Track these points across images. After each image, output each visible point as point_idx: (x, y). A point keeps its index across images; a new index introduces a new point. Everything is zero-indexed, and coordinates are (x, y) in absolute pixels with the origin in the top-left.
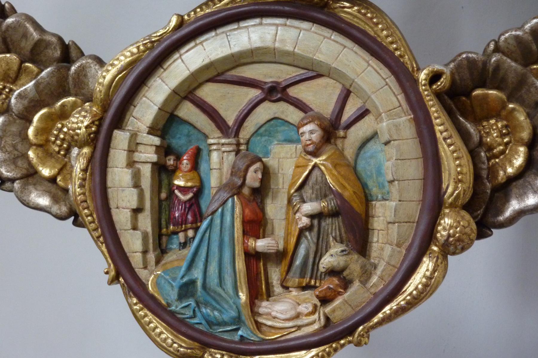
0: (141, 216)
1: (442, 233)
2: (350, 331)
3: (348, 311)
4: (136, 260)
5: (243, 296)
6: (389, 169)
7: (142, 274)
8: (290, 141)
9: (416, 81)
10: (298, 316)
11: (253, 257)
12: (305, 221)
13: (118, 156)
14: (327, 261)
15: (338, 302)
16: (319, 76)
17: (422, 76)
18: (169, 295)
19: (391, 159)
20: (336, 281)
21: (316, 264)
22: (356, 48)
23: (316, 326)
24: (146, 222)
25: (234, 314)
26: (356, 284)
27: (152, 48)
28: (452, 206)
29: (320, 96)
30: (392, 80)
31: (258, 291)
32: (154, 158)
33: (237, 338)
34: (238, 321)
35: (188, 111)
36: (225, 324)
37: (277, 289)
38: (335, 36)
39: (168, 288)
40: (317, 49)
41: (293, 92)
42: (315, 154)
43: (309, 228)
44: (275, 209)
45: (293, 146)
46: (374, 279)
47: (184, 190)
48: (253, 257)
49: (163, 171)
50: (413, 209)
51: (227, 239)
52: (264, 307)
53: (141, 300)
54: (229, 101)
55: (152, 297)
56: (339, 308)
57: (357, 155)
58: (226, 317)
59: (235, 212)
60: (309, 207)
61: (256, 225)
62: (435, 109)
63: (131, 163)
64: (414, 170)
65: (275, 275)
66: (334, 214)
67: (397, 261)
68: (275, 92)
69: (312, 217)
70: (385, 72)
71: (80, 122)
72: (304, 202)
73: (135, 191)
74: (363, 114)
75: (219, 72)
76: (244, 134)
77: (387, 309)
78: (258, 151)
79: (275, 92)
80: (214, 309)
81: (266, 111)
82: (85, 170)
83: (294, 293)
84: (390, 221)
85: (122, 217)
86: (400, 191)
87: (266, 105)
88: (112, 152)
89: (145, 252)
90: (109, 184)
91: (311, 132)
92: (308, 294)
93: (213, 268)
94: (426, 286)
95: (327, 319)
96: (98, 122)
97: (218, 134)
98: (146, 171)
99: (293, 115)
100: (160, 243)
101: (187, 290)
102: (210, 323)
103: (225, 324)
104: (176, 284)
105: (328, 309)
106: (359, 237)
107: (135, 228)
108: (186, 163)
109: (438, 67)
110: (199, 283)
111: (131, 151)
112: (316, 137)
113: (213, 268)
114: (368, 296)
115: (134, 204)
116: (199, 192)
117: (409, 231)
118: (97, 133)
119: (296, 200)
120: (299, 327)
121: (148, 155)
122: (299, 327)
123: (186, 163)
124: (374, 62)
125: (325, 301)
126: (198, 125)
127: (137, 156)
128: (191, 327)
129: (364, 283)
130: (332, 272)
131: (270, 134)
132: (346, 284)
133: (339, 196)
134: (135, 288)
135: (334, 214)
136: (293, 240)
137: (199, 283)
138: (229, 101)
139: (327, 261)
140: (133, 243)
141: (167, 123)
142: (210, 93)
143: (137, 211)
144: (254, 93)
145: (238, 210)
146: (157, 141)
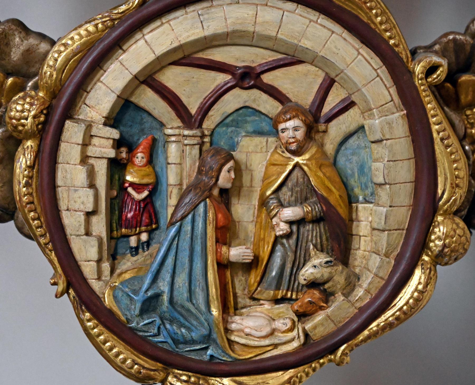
0: (94, 219)
1: (436, 244)
2: (333, 349)
3: (331, 328)
4: (89, 270)
5: (215, 312)
6: (378, 171)
7: (96, 285)
8: (260, 133)
9: (411, 73)
10: (272, 333)
11: (223, 266)
12: (283, 228)
13: (70, 150)
14: (308, 272)
15: (319, 317)
16: (300, 62)
17: (419, 69)
18: (127, 310)
19: (385, 160)
20: (317, 294)
21: (294, 275)
22: (346, 34)
23: (295, 344)
24: (99, 225)
25: (205, 332)
26: (340, 298)
27: (113, 28)
28: (445, 213)
29: (299, 84)
30: (383, 72)
31: (229, 306)
32: (112, 153)
33: (206, 358)
34: (208, 339)
35: (148, 99)
36: (193, 342)
37: (242, 301)
38: (323, 20)
39: (126, 301)
40: (303, 34)
41: (267, 78)
42: (296, 153)
43: (288, 236)
44: (244, 211)
45: (263, 140)
46: (359, 292)
47: (138, 187)
48: (223, 266)
49: (117, 166)
50: (403, 215)
51: (198, 248)
52: (237, 323)
53: (95, 315)
54: (193, 86)
55: (110, 312)
56: (319, 324)
57: (337, 151)
58: (194, 335)
59: (206, 216)
60: (290, 213)
61: (226, 232)
62: (431, 106)
63: (84, 159)
64: (405, 172)
65: (241, 284)
66: (317, 221)
67: (385, 273)
68: (247, 78)
69: (290, 223)
70: (376, 62)
71: (24, 110)
72: (281, 205)
73: (91, 192)
74: (347, 105)
75: (186, 57)
76: (208, 124)
77: (374, 325)
78: (223, 143)
79: (247, 78)
80: (181, 325)
81: (235, 99)
82: (31, 167)
83: (267, 306)
84: (375, 225)
85: (72, 222)
86: (391, 197)
87: (237, 91)
88: (63, 146)
89: (99, 261)
90: (59, 182)
91: (292, 128)
92: (282, 307)
93: (182, 280)
94: (417, 300)
95: (307, 335)
96: (48, 110)
97: (178, 123)
98: (101, 168)
99: (269, 106)
100: (113, 251)
101: (150, 304)
102: (176, 342)
103: (193, 342)
104: (139, 298)
105: (308, 326)
106: (341, 243)
107: (88, 233)
108: (140, 158)
109: (436, 59)
110: (166, 298)
111: (85, 145)
112: (300, 134)
113: (182, 280)
114: (353, 311)
115: (90, 208)
116: (155, 188)
117: (398, 238)
118: (44, 123)
119: (273, 203)
120: (276, 346)
121: (103, 147)
122: (276, 346)
123: (140, 158)
124: (365, 51)
125: (302, 316)
126: (155, 113)
127: (91, 151)
128: (154, 345)
129: (346, 295)
130: (313, 284)
131: (237, 124)
132: (328, 296)
133: (323, 200)
134: (86, 300)
135: (317, 221)
136: (267, 249)
137: (166, 298)
138: (193, 86)
139: (308, 272)
140: (86, 251)
141: (123, 112)
142: (172, 78)
143: (89, 214)
144: (222, 78)
145: (211, 215)
146: (115, 134)
